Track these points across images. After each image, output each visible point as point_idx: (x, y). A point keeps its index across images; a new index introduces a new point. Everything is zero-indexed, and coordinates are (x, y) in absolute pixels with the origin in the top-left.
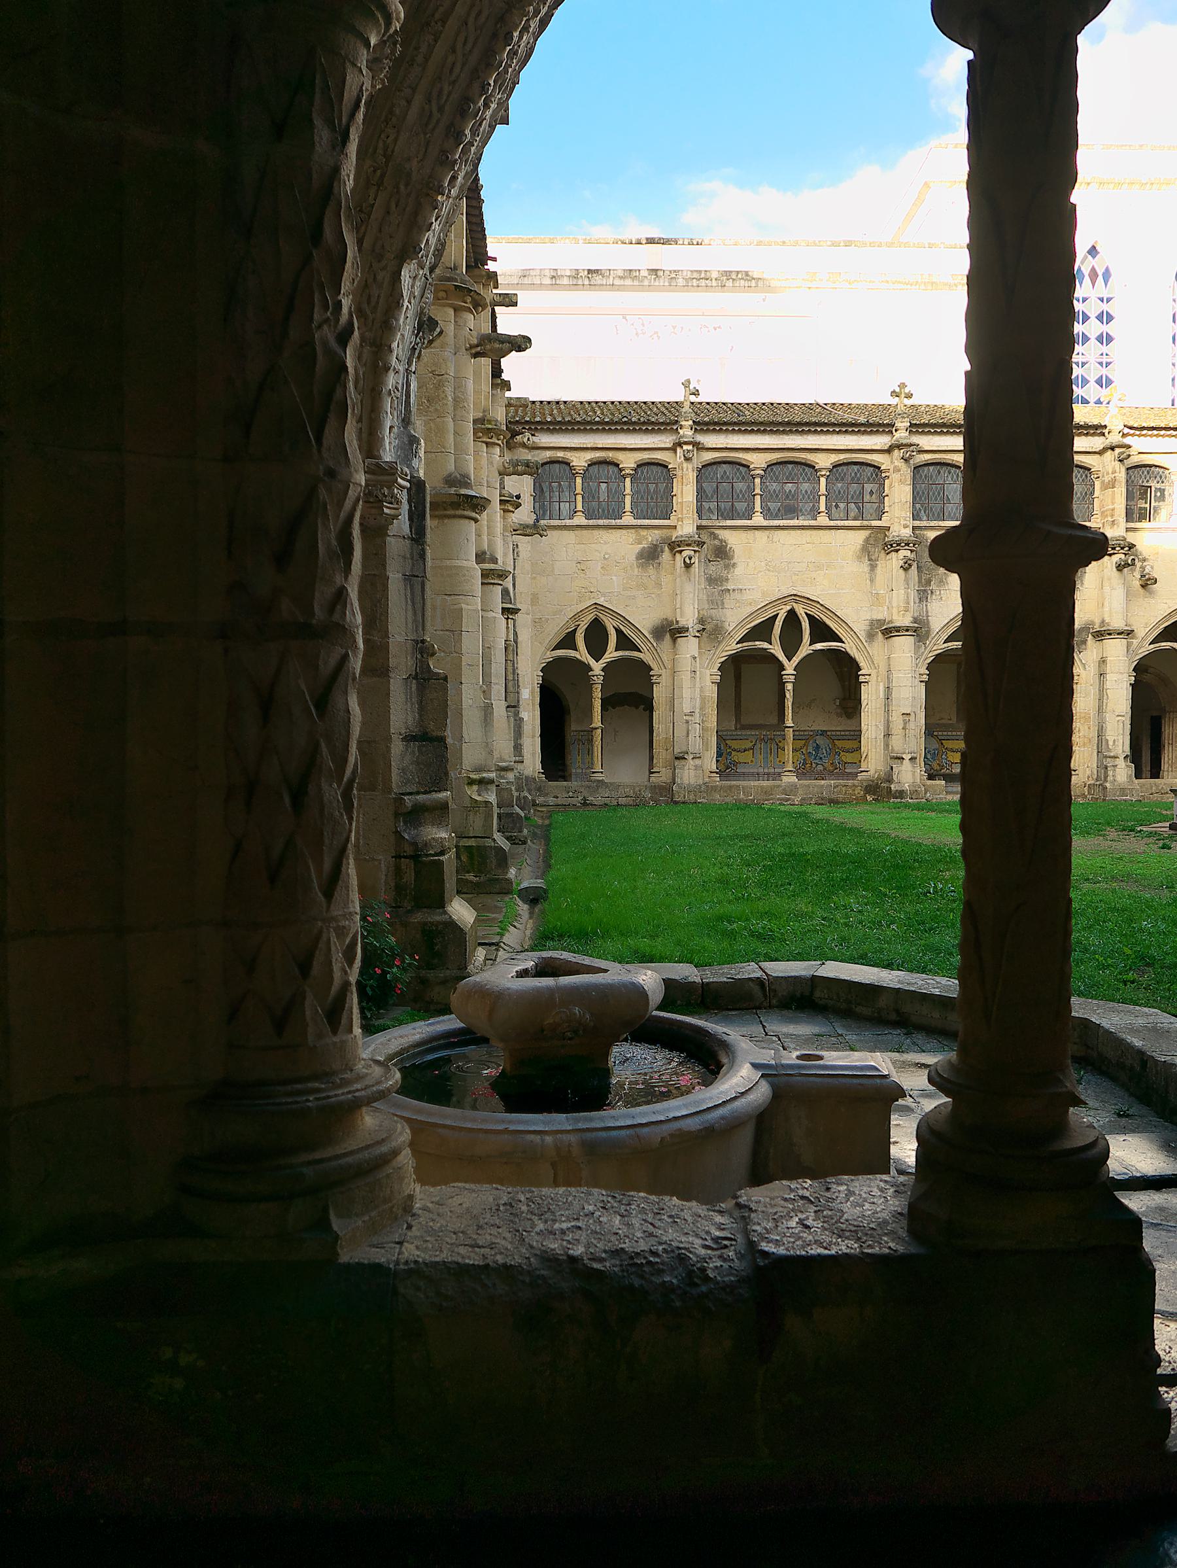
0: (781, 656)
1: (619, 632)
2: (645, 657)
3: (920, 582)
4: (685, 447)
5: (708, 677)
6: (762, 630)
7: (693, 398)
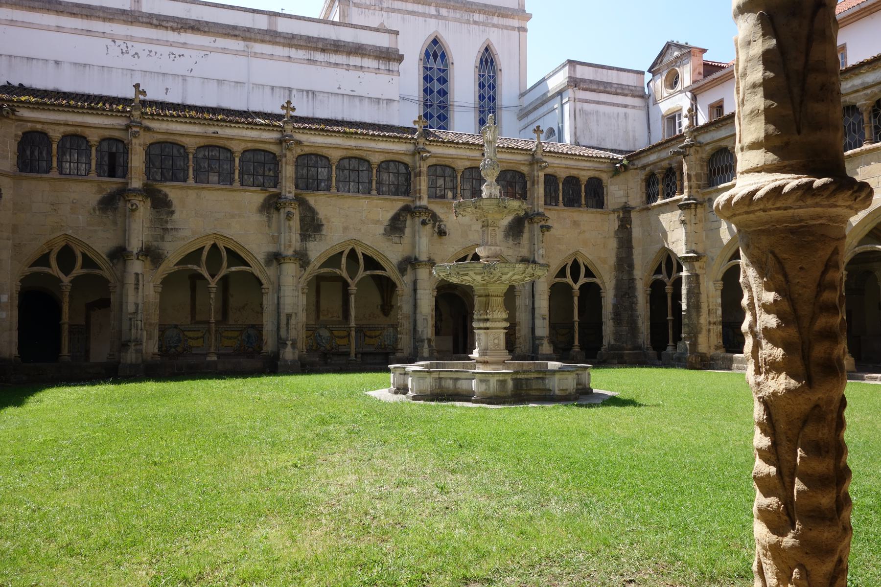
0: (206, 275)
1: (84, 255)
2: (106, 274)
3: (301, 228)
4: (134, 129)
5: (152, 288)
6: (194, 256)
7: (141, 97)
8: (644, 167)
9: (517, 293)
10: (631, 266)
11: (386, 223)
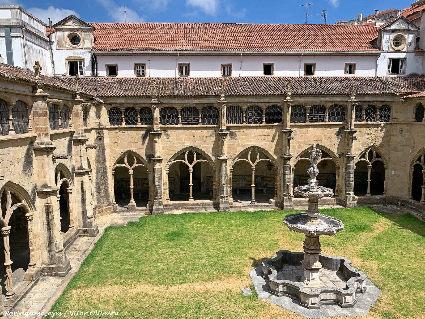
8: (110, 104)
9: (69, 191)
10: (104, 160)
11: (23, 160)
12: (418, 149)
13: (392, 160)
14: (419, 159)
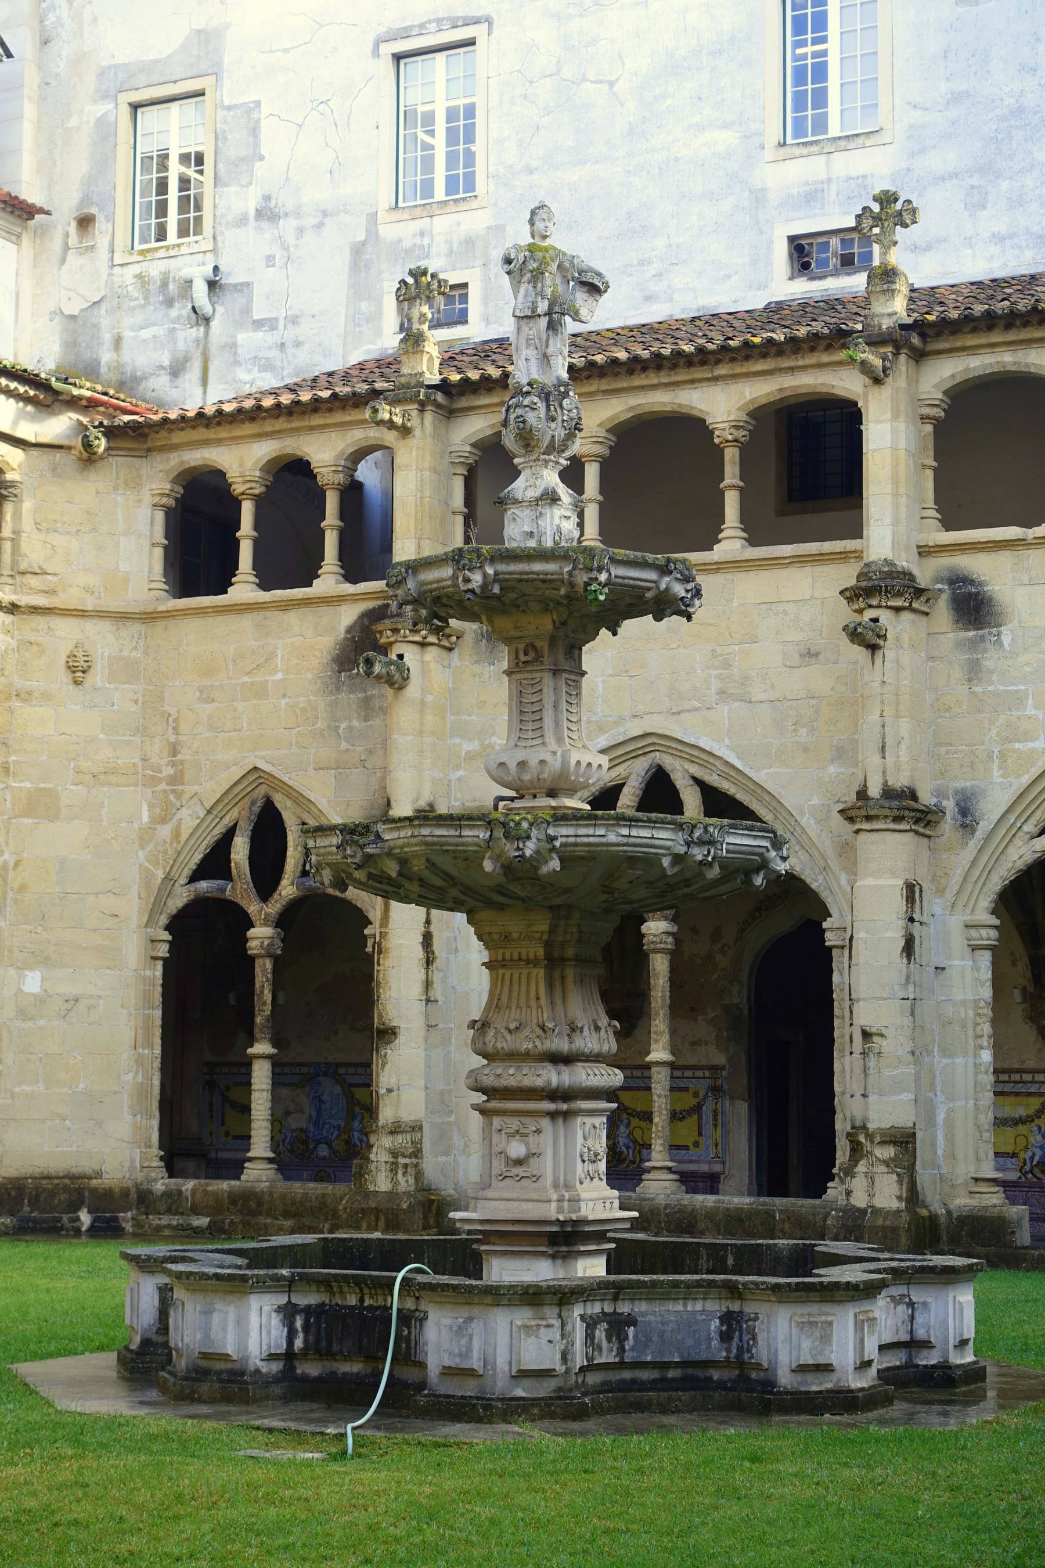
12: (212, 785)
13: (22, 888)
14: (215, 863)
